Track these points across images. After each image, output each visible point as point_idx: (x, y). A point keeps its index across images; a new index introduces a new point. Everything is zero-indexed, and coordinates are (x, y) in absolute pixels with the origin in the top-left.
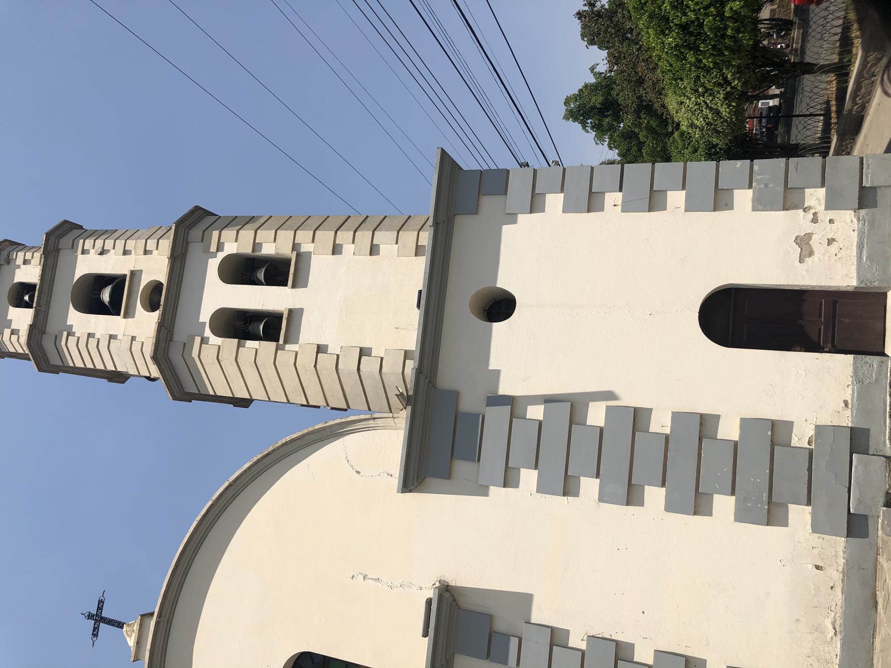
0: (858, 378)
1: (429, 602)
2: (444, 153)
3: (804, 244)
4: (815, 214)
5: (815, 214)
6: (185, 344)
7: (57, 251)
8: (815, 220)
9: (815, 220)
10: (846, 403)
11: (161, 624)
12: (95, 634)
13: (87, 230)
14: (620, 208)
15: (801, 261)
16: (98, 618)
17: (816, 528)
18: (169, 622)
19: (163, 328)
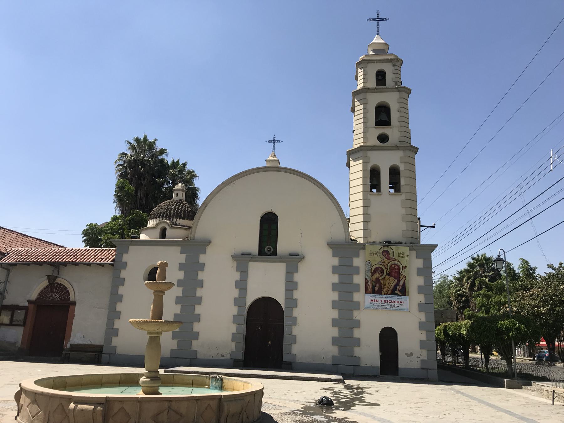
0: (374, 367)
1: (298, 255)
2: (436, 246)
3: (411, 354)
4: (420, 357)
5: (420, 357)
6: (366, 156)
7: (399, 91)
8: (418, 357)
9: (418, 357)
10: (366, 365)
11: (277, 169)
12: (270, 141)
13: (408, 100)
14: (420, 302)
15: (405, 354)
16: (274, 141)
17: (333, 357)
18: (279, 171)
19: (371, 147)
